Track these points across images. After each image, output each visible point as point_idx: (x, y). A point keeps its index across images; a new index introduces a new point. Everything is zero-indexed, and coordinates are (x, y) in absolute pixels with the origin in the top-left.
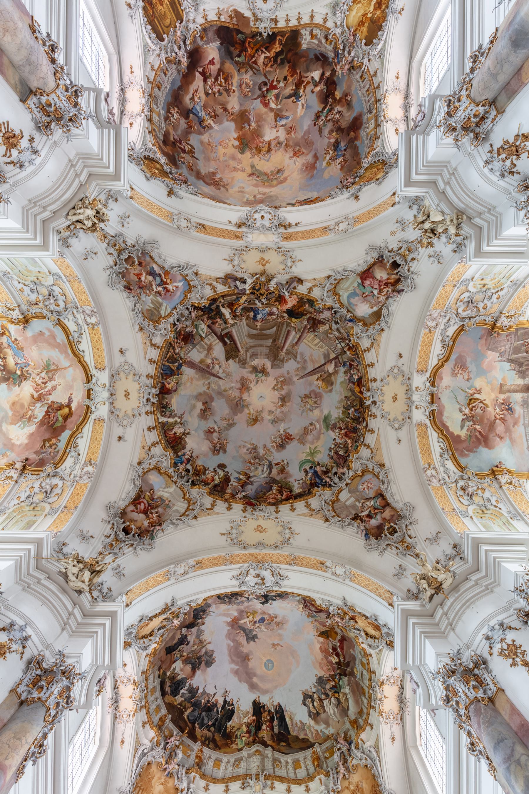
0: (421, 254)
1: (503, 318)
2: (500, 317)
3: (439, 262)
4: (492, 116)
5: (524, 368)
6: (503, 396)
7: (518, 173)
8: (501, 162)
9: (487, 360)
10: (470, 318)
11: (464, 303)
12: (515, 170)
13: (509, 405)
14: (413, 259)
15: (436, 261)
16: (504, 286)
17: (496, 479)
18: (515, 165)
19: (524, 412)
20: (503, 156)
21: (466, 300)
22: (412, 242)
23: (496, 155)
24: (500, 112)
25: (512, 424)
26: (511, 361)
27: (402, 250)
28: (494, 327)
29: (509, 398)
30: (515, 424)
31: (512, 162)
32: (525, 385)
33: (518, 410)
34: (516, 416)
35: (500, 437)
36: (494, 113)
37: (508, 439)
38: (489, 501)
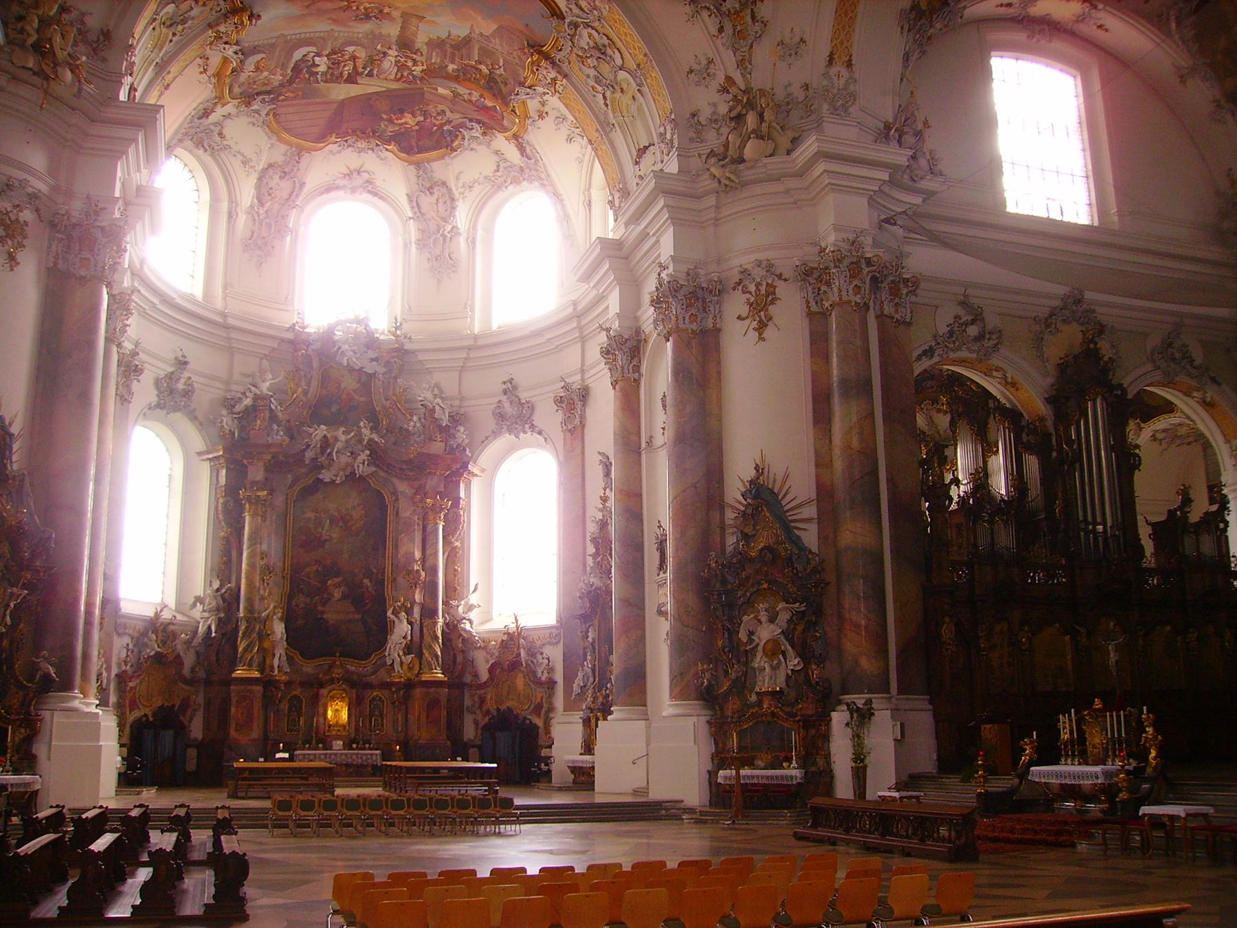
0: (722, 49)
1: (553, 74)
2: (558, 72)
3: (691, 71)
4: (812, 303)
5: (449, 50)
6: (396, 14)
7: (734, 289)
8: (759, 280)
9: (479, 18)
10: (573, 36)
11: (604, 46)
12: (740, 288)
13: (377, 18)
14: (721, 30)
15: (696, 67)
16: (610, 112)
17: (226, 16)
18: (744, 292)
19: (359, 33)
20: (763, 289)
21: (609, 51)
22: (751, 46)
23: (770, 281)
24: (811, 315)
25: (334, 17)
26: (467, 41)
27: (749, 19)
28: (547, 57)
29: (392, 19)
30: (335, 21)
31: (750, 293)
32: (413, 42)
33: (365, 28)
34: (351, 24)
35: (307, 7)
36: (814, 308)
37: (304, 12)
38: (184, 22)
